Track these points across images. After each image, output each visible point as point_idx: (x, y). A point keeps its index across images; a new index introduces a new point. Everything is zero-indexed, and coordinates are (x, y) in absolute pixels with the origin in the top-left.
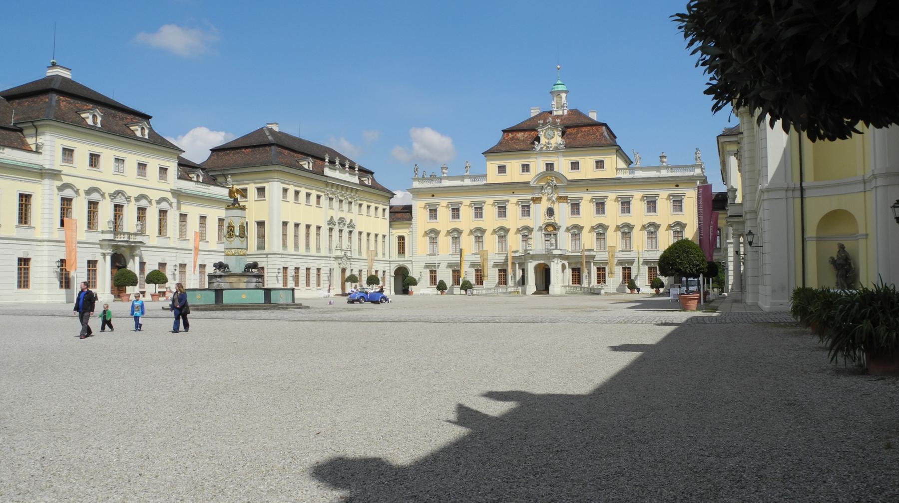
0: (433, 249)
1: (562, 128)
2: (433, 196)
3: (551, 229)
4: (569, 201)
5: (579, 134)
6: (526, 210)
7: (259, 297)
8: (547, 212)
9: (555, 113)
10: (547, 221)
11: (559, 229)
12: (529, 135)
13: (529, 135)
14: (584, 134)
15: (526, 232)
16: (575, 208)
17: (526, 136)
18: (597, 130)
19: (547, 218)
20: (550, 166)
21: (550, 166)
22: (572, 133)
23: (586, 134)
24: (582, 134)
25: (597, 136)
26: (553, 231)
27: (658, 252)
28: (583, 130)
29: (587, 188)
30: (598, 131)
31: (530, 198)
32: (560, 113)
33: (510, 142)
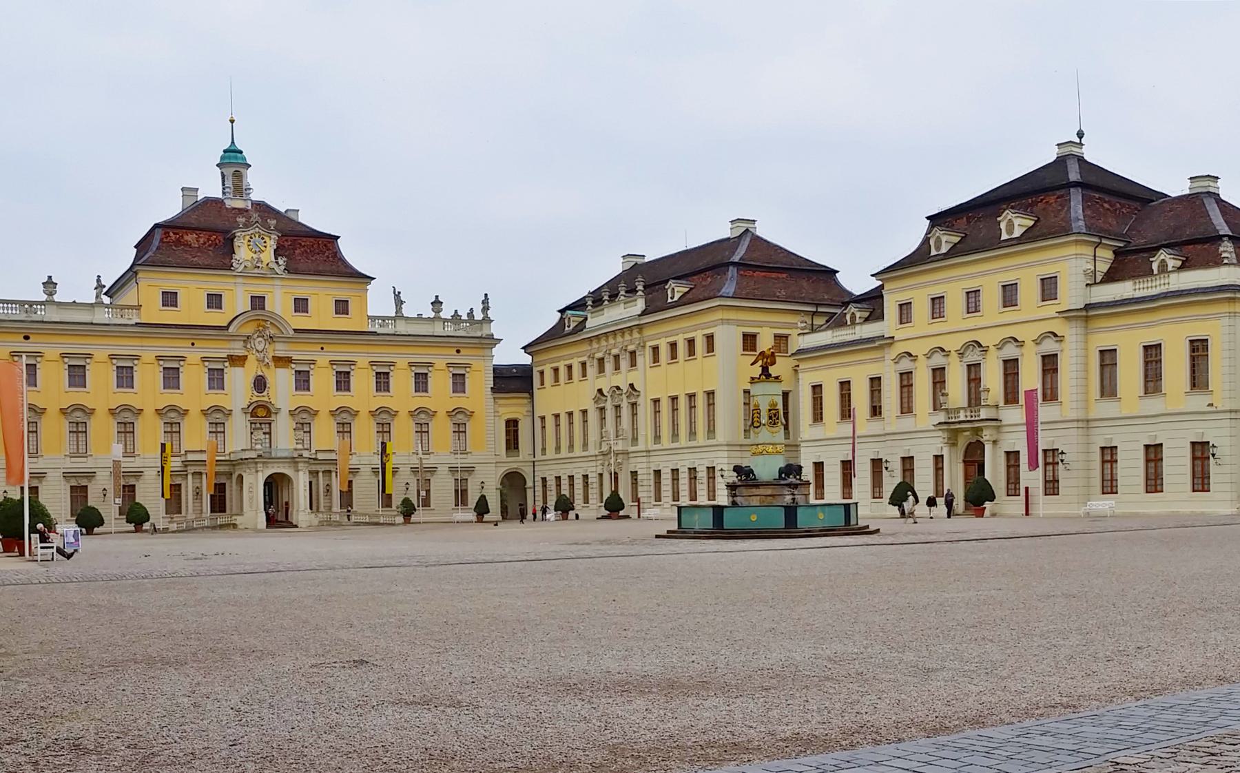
0: (78, 443)
1: (278, 236)
2: (27, 338)
3: (261, 414)
4: (293, 366)
5: (296, 249)
6: (216, 379)
7: (778, 519)
8: (254, 384)
9: (230, 204)
10: (255, 399)
11: (276, 413)
12: (209, 240)
13: (209, 240)
14: (306, 252)
15: (217, 418)
16: (303, 381)
17: (202, 241)
18: (325, 245)
19: (256, 394)
20: (258, 302)
21: (258, 302)
22: (285, 247)
23: (309, 251)
24: (302, 250)
25: (328, 257)
26: (265, 417)
27: (432, 455)
28: (303, 244)
29: (322, 346)
30: (329, 249)
31: (225, 355)
32: (239, 204)
33: (174, 247)
